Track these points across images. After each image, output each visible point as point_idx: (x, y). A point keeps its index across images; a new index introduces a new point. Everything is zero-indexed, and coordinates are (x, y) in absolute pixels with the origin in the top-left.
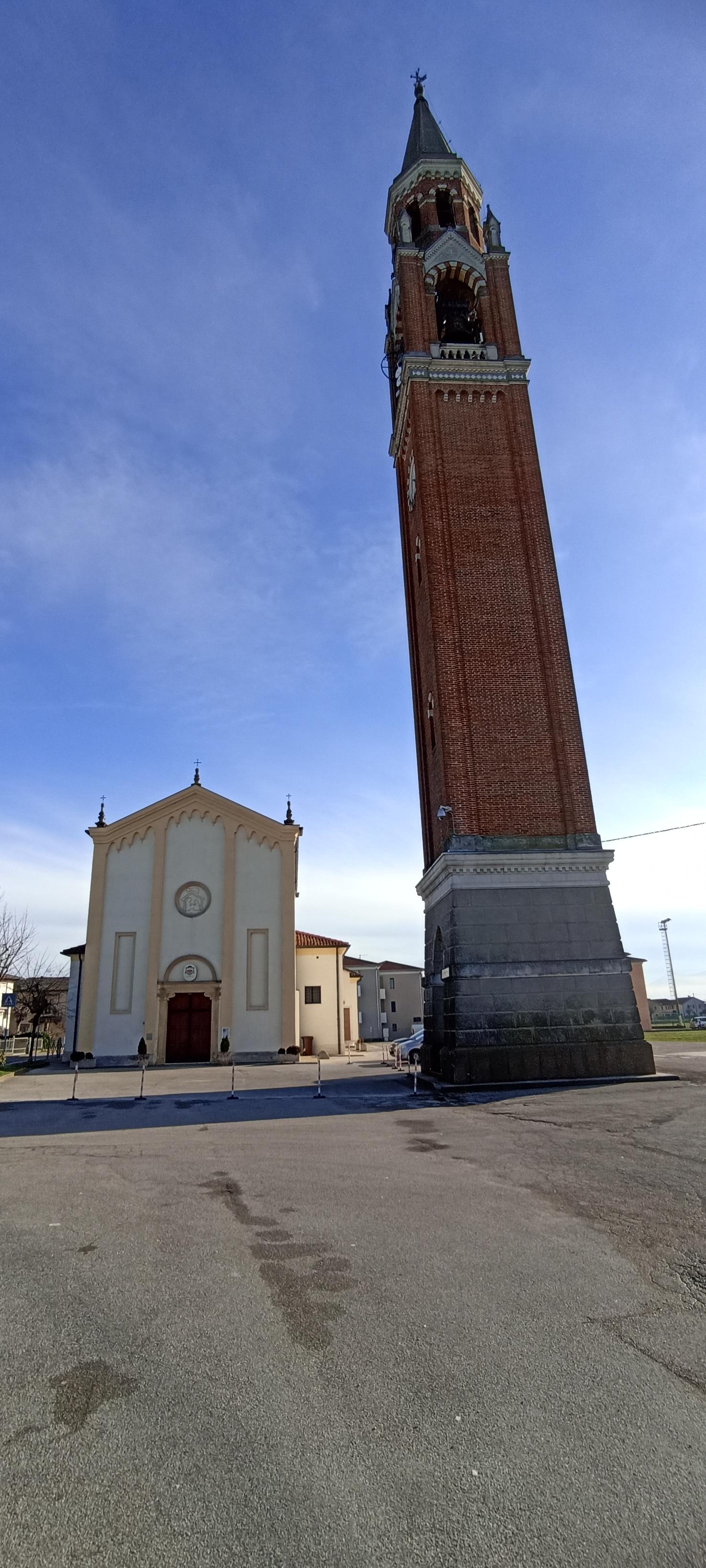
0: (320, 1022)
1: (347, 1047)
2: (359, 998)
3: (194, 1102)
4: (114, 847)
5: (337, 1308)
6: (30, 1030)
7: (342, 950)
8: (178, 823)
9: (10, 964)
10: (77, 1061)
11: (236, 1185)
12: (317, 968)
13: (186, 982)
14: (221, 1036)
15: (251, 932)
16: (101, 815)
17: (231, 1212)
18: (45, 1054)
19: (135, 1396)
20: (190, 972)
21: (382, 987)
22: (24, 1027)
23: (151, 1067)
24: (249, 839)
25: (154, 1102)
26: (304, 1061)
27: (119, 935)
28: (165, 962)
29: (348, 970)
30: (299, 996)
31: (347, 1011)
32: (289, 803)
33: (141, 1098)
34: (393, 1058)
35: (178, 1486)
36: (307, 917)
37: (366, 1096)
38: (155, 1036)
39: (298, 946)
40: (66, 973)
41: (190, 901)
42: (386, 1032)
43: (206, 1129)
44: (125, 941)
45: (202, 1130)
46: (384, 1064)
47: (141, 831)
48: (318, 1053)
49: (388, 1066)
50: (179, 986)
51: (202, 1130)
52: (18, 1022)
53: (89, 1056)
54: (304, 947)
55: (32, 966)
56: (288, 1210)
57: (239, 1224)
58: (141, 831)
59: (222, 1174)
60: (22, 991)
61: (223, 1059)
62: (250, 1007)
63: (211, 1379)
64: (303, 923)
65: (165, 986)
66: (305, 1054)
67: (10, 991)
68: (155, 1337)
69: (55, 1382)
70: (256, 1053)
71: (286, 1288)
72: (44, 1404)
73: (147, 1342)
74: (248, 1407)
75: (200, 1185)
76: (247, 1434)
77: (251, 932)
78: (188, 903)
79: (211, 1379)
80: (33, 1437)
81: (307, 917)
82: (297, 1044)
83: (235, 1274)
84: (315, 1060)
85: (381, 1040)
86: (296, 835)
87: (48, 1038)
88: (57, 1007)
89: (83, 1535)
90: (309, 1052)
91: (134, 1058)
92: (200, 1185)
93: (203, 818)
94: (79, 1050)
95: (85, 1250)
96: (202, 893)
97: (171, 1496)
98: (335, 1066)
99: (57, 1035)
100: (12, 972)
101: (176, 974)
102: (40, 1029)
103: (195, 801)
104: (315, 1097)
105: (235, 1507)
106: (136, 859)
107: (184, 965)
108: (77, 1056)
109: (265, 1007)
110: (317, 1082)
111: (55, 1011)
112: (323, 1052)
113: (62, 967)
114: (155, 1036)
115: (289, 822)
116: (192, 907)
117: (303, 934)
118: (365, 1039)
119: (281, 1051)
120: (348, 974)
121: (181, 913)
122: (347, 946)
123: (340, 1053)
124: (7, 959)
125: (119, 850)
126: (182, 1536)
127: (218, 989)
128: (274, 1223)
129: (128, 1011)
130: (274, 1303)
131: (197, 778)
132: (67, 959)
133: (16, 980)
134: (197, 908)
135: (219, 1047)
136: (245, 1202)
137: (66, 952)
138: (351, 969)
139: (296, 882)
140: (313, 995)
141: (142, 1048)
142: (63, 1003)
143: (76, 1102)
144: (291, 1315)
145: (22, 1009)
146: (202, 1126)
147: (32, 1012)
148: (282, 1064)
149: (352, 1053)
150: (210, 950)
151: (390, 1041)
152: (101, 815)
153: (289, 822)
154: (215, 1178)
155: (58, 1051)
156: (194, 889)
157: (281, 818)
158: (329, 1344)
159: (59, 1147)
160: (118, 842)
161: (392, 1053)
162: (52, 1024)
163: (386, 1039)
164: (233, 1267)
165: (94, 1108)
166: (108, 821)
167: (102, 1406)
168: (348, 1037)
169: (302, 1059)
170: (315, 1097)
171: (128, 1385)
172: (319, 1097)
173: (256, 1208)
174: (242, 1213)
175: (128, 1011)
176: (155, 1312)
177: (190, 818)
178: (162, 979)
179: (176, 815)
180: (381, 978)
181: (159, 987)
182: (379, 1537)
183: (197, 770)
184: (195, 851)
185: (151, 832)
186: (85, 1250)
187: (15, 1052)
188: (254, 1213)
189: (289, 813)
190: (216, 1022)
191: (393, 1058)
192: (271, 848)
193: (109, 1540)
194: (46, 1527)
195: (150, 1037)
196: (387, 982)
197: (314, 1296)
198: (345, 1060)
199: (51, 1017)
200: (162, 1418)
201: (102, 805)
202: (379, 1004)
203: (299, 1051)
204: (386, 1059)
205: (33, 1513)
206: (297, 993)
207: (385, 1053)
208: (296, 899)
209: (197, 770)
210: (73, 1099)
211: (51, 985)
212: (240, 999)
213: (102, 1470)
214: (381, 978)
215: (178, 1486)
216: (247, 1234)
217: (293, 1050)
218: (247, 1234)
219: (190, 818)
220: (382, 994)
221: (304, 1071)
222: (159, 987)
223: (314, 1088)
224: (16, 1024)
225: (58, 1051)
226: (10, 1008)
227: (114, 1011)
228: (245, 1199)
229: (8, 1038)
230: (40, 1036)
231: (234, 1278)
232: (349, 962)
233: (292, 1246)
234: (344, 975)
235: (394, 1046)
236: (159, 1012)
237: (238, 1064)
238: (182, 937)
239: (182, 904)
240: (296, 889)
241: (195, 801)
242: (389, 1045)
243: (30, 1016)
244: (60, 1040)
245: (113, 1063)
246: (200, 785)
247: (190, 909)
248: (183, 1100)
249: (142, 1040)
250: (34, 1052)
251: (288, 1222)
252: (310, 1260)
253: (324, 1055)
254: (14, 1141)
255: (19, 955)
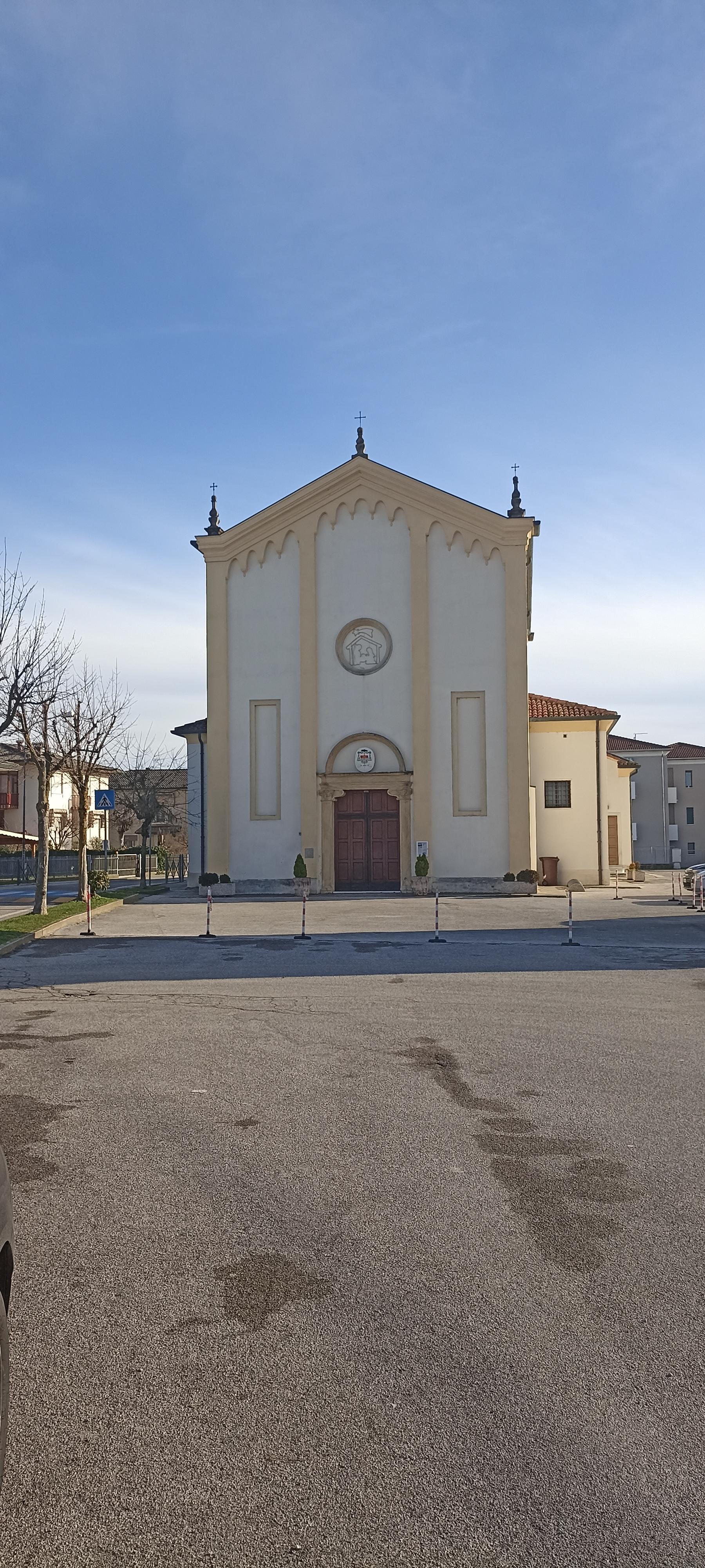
0: (569, 833)
1: (613, 875)
2: (632, 801)
3: (381, 944)
4: (237, 567)
5: (609, 1224)
6: (138, 844)
7: (606, 724)
8: (334, 524)
9: (101, 747)
10: (210, 885)
11: (449, 1057)
12: (566, 752)
13: (360, 774)
14: (416, 853)
15: (457, 697)
16: (213, 515)
17: (444, 1091)
18: (163, 877)
19: (327, 1299)
20: (364, 758)
21: (671, 785)
22: (129, 840)
23: (314, 896)
24: (449, 545)
25: (324, 942)
26: (545, 893)
27: (256, 704)
28: (327, 744)
29: (615, 757)
30: (535, 796)
31: (613, 819)
32: (515, 480)
33: (303, 936)
34: (690, 893)
35: (394, 1406)
36: (549, 671)
37: (647, 946)
38: (318, 852)
39: (534, 718)
40: (182, 762)
41: (359, 649)
42: (677, 854)
43: (401, 981)
44: (265, 712)
45: (393, 982)
46: (673, 901)
47: (278, 539)
48: (566, 882)
49: (681, 904)
50: (350, 779)
51: (393, 982)
52: (121, 832)
53: (225, 879)
54: (544, 719)
55: (133, 751)
56: (528, 1093)
57: (458, 1108)
58: (278, 539)
59: (427, 1040)
60: (120, 788)
61: (420, 887)
62: (458, 811)
63: (429, 1290)
64: (542, 681)
65: (328, 780)
66: (546, 883)
67: (104, 787)
68: (348, 1235)
69: (221, 1273)
70: (470, 880)
71: (532, 1195)
72: (209, 1296)
73: (339, 1239)
74: (485, 1329)
75: (399, 1054)
76: (485, 1360)
77: (457, 697)
78: (356, 653)
79: (429, 1290)
80: (200, 1329)
81: (549, 671)
82: (534, 867)
83: (456, 1169)
84: (563, 892)
85: (670, 867)
86: (529, 536)
87: (164, 855)
88: (174, 811)
89: (277, 1440)
90: (552, 882)
91: (289, 883)
92: (399, 1054)
93: (373, 513)
94: (209, 871)
95: (244, 1124)
96: (378, 636)
97: (386, 1415)
98: (592, 902)
99: (177, 851)
100: (105, 760)
101: (346, 761)
102: (153, 842)
103: (360, 484)
104: (563, 944)
105: (473, 1437)
106: (271, 584)
107: (355, 748)
108: (208, 879)
109: (481, 811)
110: (566, 923)
111: (172, 817)
112: (575, 881)
113: (174, 753)
114: (318, 852)
115: (516, 512)
116: (364, 658)
117: (541, 698)
118: (641, 865)
119: (509, 877)
120: (615, 763)
121: (347, 669)
122: (615, 717)
123: (601, 884)
124: (96, 740)
125: (245, 572)
126: (405, 1459)
127: (408, 784)
128: (510, 1109)
129: (276, 816)
130: (513, 1209)
131: (360, 444)
132: (182, 741)
133: (111, 773)
134: (370, 660)
135: (414, 870)
136: (464, 1079)
137: (178, 731)
138: (622, 755)
139: (529, 613)
140: (558, 794)
141: (300, 868)
142: (181, 806)
143: (211, 940)
144: (541, 1227)
145: (125, 813)
146: (394, 976)
147: (139, 818)
148: (509, 896)
149: (620, 884)
150: (392, 722)
151: (683, 868)
152: (213, 515)
153: (516, 512)
154: (419, 1045)
155: (181, 875)
156: (366, 630)
157: (504, 507)
158: (598, 1266)
159: (194, 996)
160: (242, 559)
161: (687, 885)
162: (169, 836)
163: (676, 865)
164: (451, 1159)
165: (238, 948)
166: (224, 524)
167: (286, 1306)
168: (614, 860)
169: (541, 890)
170: (563, 944)
171: (316, 1288)
172: (571, 943)
173: (480, 1087)
174: (460, 1093)
175: (276, 816)
176: (347, 1206)
177: (352, 514)
178: (323, 770)
179: (331, 509)
180: (670, 770)
181: (320, 780)
182: (680, 1499)
183: (360, 431)
184: (363, 565)
185: (293, 538)
186: (244, 1124)
187: (121, 873)
188: (478, 1094)
189: (516, 496)
190: (408, 834)
191: (690, 893)
192: (487, 559)
193: (311, 1449)
194: (230, 1425)
195: (310, 854)
196: (680, 777)
197: (574, 1205)
198: (612, 893)
199: (166, 826)
200: (366, 1328)
201: (214, 499)
202: (665, 811)
203: (537, 879)
204: (677, 893)
205: (211, 1408)
206: (532, 790)
207: (676, 885)
208: (529, 643)
209: (360, 431)
210: (208, 935)
211: (162, 779)
212: (442, 801)
213: (293, 1376)
214: (670, 770)
215: (394, 1406)
216: (471, 1121)
217: (527, 876)
218: (471, 1121)
219: (352, 514)
220: (672, 795)
221: (546, 906)
222: (320, 780)
223: (565, 931)
224: (118, 835)
225: (181, 875)
226: (107, 812)
227: (255, 815)
228: (465, 1076)
229: (109, 853)
230: (154, 853)
231: (454, 1174)
232: (617, 744)
233: (538, 1140)
234: (609, 764)
235: (691, 874)
236: (322, 818)
237: (442, 895)
238: (352, 706)
239: (347, 654)
240: (529, 628)
241: (360, 484)
242: (683, 874)
243: (138, 824)
244: (181, 858)
245: (259, 890)
246: (366, 456)
247: (360, 662)
248: (363, 941)
249: (299, 857)
250: (147, 874)
251: (529, 1109)
252: (565, 1161)
253: (576, 886)
254: (132, 987)
255: (115, 732)
